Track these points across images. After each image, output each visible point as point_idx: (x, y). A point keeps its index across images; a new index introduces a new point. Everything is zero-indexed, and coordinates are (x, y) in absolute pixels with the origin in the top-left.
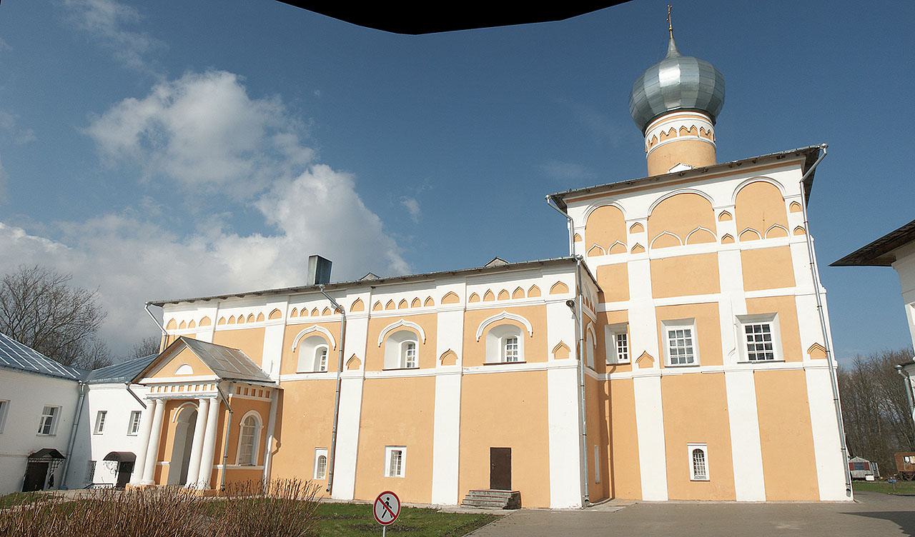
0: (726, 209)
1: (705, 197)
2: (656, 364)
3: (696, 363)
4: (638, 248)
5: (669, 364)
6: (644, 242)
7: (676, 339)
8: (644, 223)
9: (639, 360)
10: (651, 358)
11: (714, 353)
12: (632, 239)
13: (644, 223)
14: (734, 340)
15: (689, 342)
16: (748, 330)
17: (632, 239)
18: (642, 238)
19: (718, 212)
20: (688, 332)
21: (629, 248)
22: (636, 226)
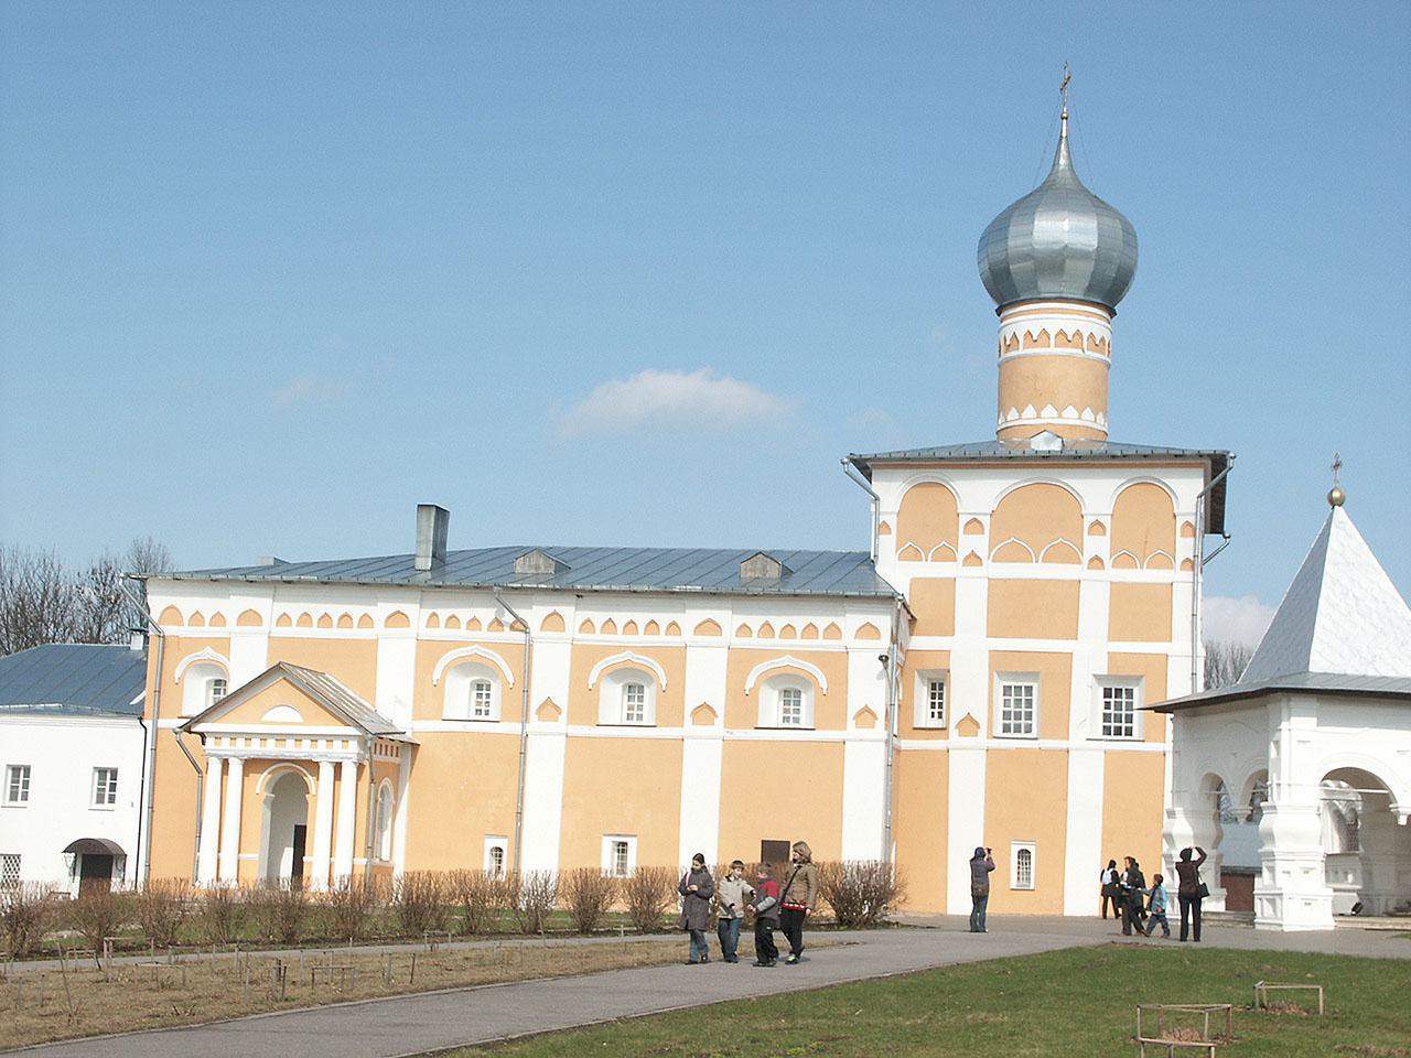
0: (1098, 518)
1: (1074, 498)
2: (983, 731)
3: (1034, 734)
4: (973, 559)
5: (999, 731)
6: (982, 552)
7: (1012, 698)
8: (986, 521)
9: (959, 725)
10: (977, 725)
11: (1059, 723)
12: (968, 543)
13: (986, 521)
14: (1087, 707)
15: (1029, 703)
16: (1107, 693)
17: (968, 543)
18: (979, 543)
19: (1088, 521)
20: (1029, 690)
21: (961, 556)
22: (974, 525)
